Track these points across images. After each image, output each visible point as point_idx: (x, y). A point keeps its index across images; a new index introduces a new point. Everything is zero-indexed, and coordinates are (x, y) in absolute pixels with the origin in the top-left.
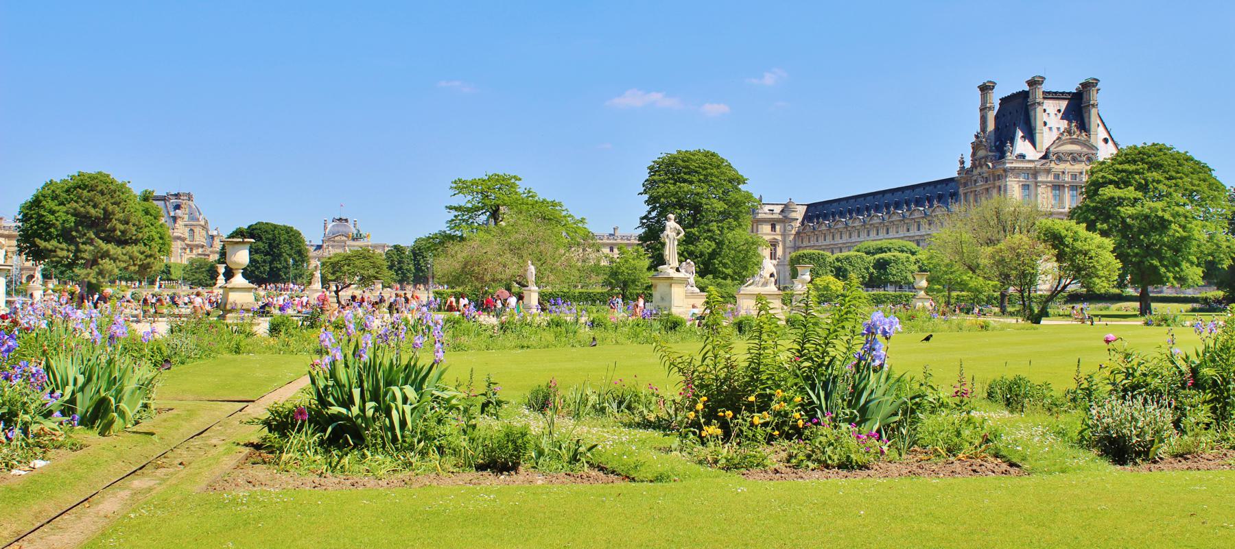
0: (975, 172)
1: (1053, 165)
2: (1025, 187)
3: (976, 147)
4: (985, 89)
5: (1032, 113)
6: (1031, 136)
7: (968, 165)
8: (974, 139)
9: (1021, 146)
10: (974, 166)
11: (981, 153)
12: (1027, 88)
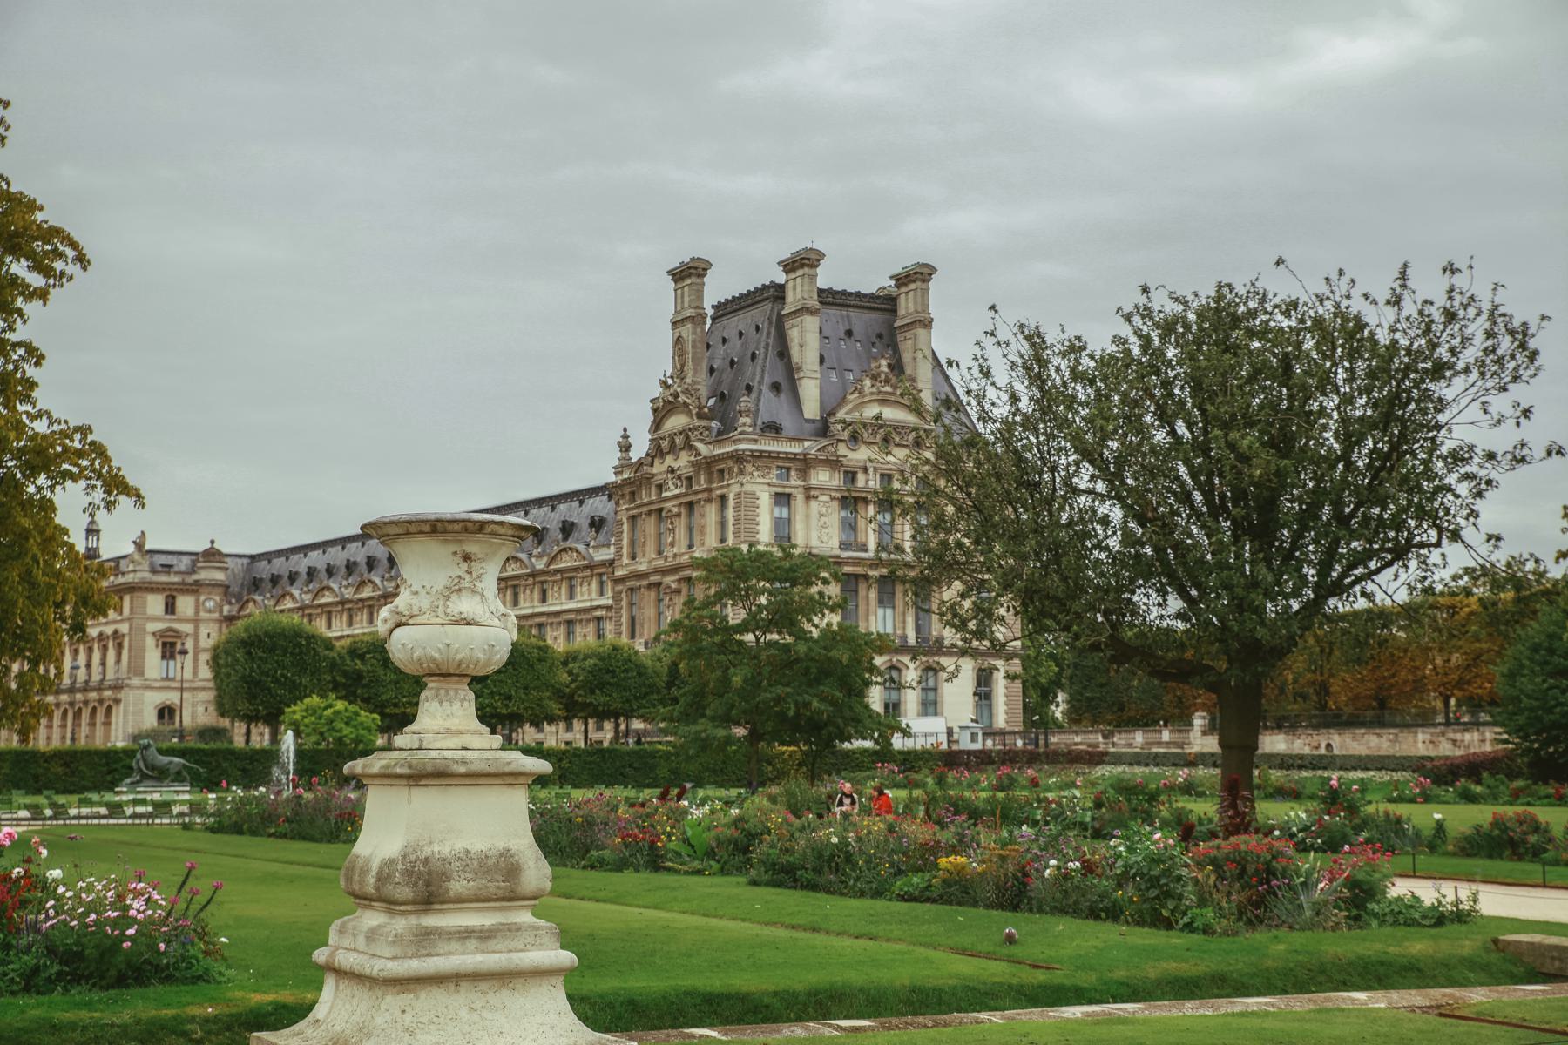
0: (659, 468)
1: (842, 450)
2: (783, 499)
3: (662, 411)
4: (689, 273)
5: (794, 334)
6: (787, 384)
7: (639, 451)
8: (657, 391)
9: (772, 407)
10: (657, 452)
11: (676, 422)
12: (780, 278)
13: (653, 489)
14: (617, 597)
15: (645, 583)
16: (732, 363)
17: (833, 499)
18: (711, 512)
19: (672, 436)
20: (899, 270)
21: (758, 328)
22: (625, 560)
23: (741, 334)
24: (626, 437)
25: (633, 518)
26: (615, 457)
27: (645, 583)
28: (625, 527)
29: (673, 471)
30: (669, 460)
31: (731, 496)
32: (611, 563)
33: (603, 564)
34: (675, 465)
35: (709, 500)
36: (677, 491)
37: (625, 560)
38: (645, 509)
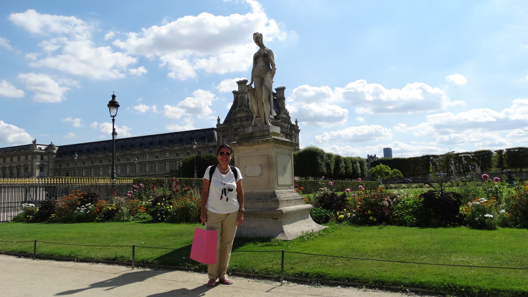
7: (222, 122)
13: (233, 130)
26: (216, 123)
30: (239, 123)
34: (243, 124)
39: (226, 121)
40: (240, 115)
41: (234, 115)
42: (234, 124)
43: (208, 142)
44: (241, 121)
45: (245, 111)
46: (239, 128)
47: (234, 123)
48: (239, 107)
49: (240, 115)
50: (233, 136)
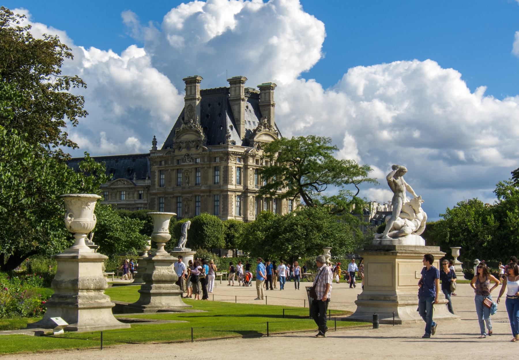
5: (235, 107)
12: (228, 86)
13: (175, 161)
14: (153, 200)
15: (172, 196)
16: (208, 116)
17: (253, 169)
18: (211, 172)
19: (188, 142)
20: (261, 84)
21: (219, 104)
22: (157, 186)
23: (209, 105)
24: (155, 139)
25: (161, 172)
27: (172, 196)
28: (157, 174)
29: (188, 155)
30: (184, 151)
31: (222, 167)
32: (148, 188)
33: (142, 187)
35: (210, 167)
36: (191, 163)
37: (157, 186)
38: (171, 168)
39: (165, 147)
40: (186, 137)
41: (178, 137)
42: (177, 152)
43: (138, 178)
44: (188, 148)
45: (193, 131)
46: (184, 160)
47: (176, 151)
48: (186, 124)
49: (186, 137)
50: (175, 172)
